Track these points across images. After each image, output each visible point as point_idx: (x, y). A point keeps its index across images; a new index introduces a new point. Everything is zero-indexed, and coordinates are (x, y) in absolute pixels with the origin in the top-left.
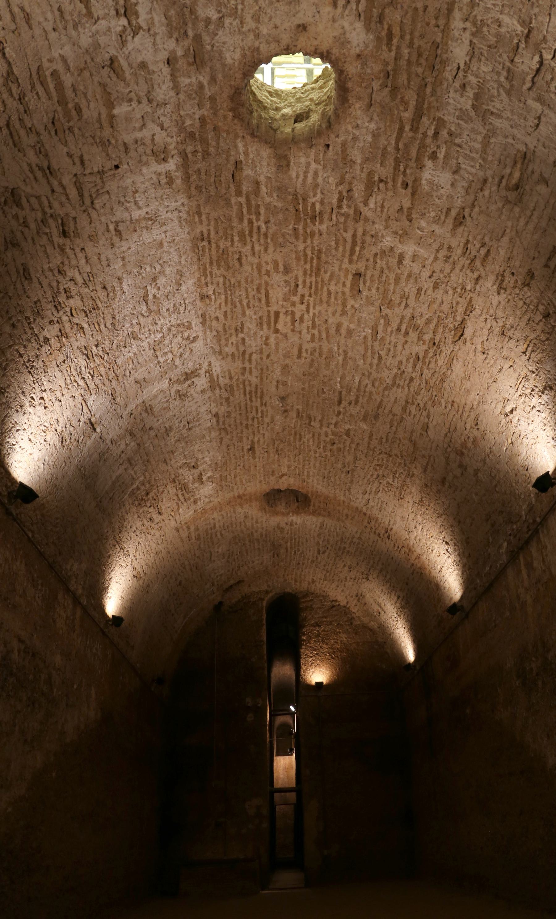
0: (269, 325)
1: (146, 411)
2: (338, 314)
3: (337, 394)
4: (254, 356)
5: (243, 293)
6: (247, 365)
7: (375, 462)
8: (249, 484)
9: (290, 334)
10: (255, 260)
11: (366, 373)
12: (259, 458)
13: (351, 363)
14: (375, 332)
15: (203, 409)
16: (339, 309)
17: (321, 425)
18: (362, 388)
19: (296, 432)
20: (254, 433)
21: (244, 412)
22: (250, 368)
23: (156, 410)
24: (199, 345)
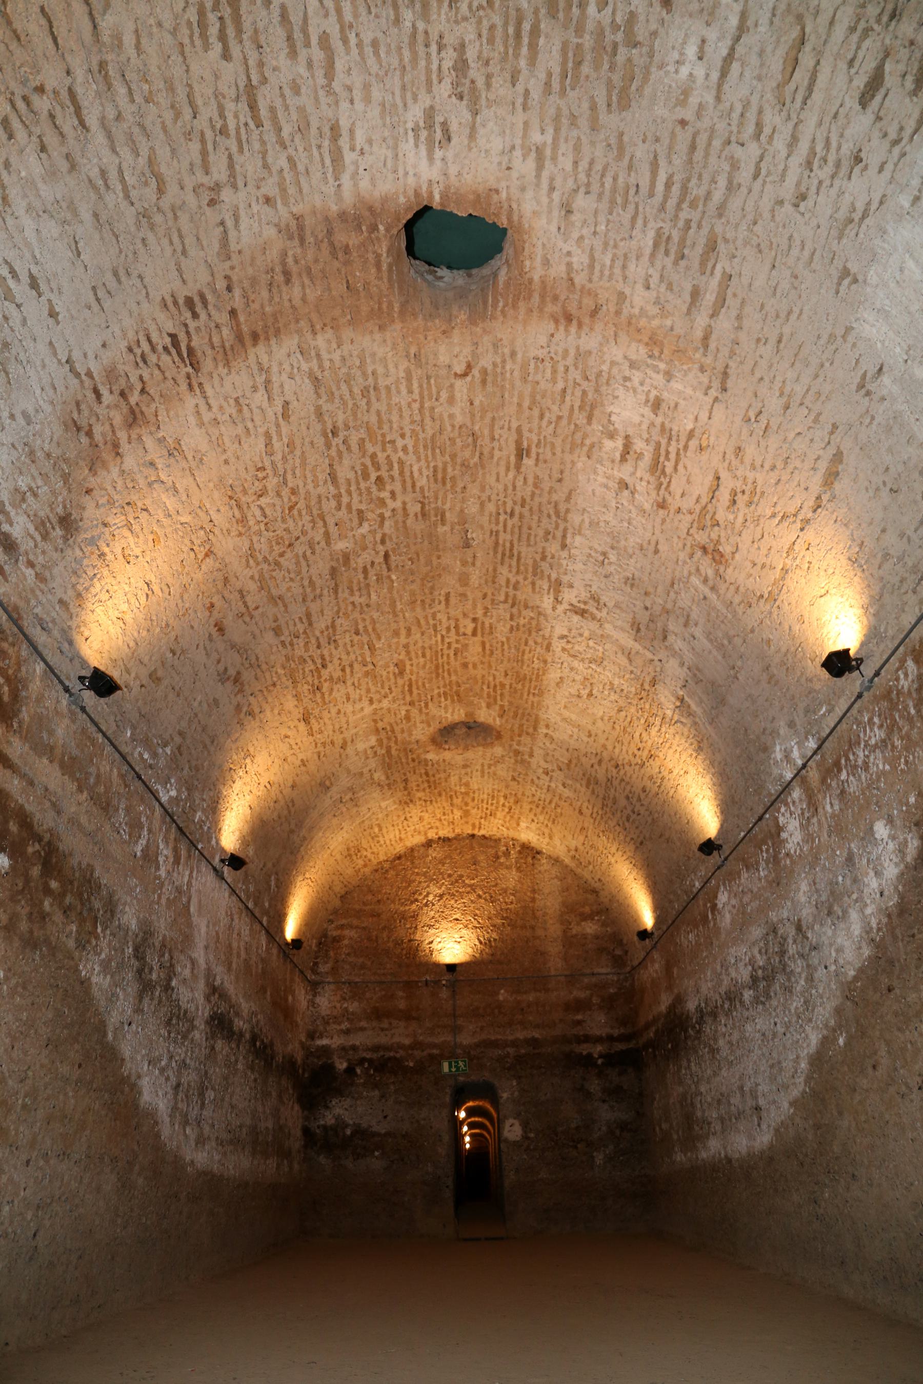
0: (483, 628)
1: (638, 630)
2: (412, 643)
3: (393, 565)
4: (502, 598)
5: (506, 653)
7: (301, 505)
8: (541, 353)
9: (460, 617)
11: (365, 609)
12: (509, 429)
13: (387, 609)
14: (372, 648)
16: (411, 648)
17: (404, 509)
18: (364, 592)
19: (444, 483)
20: (514, 488)
22: (507, 587)
23: (629, 618)
24: (560, 630)
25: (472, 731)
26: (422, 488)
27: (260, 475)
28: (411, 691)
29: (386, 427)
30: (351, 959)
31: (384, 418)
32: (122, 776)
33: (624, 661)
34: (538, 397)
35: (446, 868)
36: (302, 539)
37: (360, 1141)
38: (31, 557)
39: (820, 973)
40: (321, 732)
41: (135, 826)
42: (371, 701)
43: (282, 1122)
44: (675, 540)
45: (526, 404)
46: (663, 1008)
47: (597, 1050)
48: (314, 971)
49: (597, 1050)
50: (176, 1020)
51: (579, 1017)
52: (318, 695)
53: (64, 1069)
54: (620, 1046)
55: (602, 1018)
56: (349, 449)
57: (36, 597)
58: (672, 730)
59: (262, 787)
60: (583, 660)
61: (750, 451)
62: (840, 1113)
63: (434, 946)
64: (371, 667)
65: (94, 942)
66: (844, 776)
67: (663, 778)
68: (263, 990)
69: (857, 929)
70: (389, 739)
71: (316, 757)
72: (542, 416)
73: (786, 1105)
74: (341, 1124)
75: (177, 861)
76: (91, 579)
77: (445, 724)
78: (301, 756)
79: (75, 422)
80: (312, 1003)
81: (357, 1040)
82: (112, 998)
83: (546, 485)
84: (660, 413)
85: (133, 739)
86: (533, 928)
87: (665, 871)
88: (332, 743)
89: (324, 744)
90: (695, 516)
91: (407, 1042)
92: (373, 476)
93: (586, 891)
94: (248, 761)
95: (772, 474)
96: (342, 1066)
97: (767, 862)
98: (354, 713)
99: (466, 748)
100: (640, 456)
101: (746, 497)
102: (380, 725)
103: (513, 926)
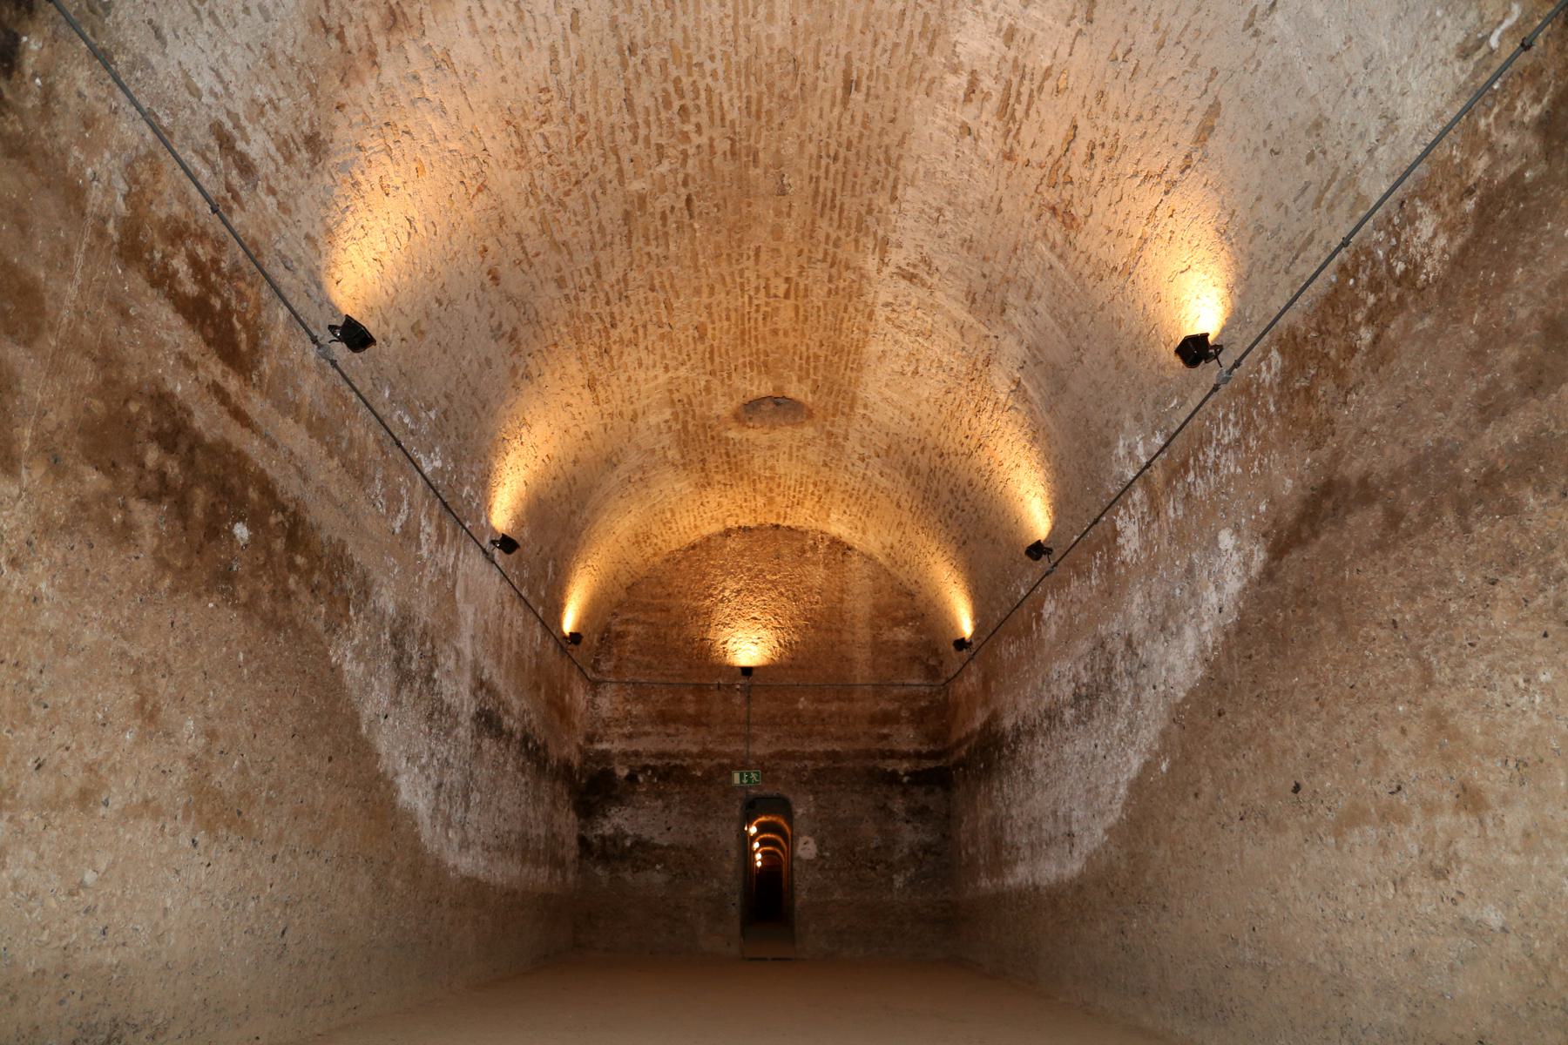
0: (797, 290)
1: (974, 301)
4: (820, 256)
6: (831, 250)
7: (592, 135)
9: (772, 275)
10: (806, 341)
12: (837, 56)
13: (687, 262)
14: (669, 307)
15: (909, 223)
16: (714, 309)
17: (711, 146)
18: (662, 241)
19: (758, 118)
20: (840, 127)
21: (850, 177)
24: (884, 296)
25: (781, 407)
26: (732, 122)
27: (544, 97)
28: (712, 359)
29: (693, 46)
30: (637, 657)
31: (691, 34)
32: (379, 442)
33: (956, 336)
34: (872, 19)
35: (746, 561)
36: (591, 175)
37: (641, 853)
38: (272, 183)
39: (1148, 693)
40: (608, 402)
41: (394, 499)
42: (666, 368)
43: (555, 829)
44: (1022, 198)
45: (858, 26)
46: (977, 725)
47: (904, 766)
48: (594, 669)
49: (904, 766)
50: (438, 715)
51: (885, 731)
52: (606, 359)
53: (312, 762)
54: (929, 764)
55: (911, 733)
56: (648, 70)
57: (278, 231)
58: (1005, 417)
59: (539, 461)
60: (909, 332)
61: (1114, 97)
62: (1157, 843)
63: (729, 646)
64: (667, 328)
65: (346, 626)
66: (1191, 477)
67: (992, 471)
68: (537, 687)
69: (1190, 647)
70: (686, 412)
71: (601, 429)
72: (875, 43)
73: (1100, 832)
74: (620, 834)
75: (441, 539)
76: (343, 212)
77: (749, 398)
78: (585, 428)
79: (323, 22)
80: (592, 704)
81: (641, 745)
82: (366, 688)
83: (876, 126)
84: (1014, 45)
85: (392, 399)
86: (839, 631)
87: (988, 575)
88: (621, 414)
89: (611, 415)
90: (1046, 171)
91: (695, 749)
92: (676, 105)
93: (900, 594)
94: (524, 430)
95: (1137, 125)
96: (622, 772)
97: (1100, 570)
98: (648, 381)
99: (773, 427)
100: (987, 96)
101: (1105, 152)
102: (676, 396)
103: (817, 628)
